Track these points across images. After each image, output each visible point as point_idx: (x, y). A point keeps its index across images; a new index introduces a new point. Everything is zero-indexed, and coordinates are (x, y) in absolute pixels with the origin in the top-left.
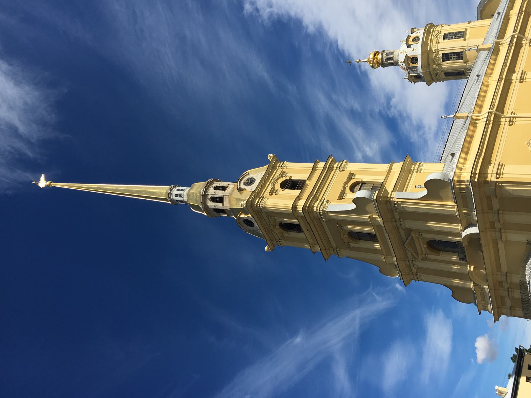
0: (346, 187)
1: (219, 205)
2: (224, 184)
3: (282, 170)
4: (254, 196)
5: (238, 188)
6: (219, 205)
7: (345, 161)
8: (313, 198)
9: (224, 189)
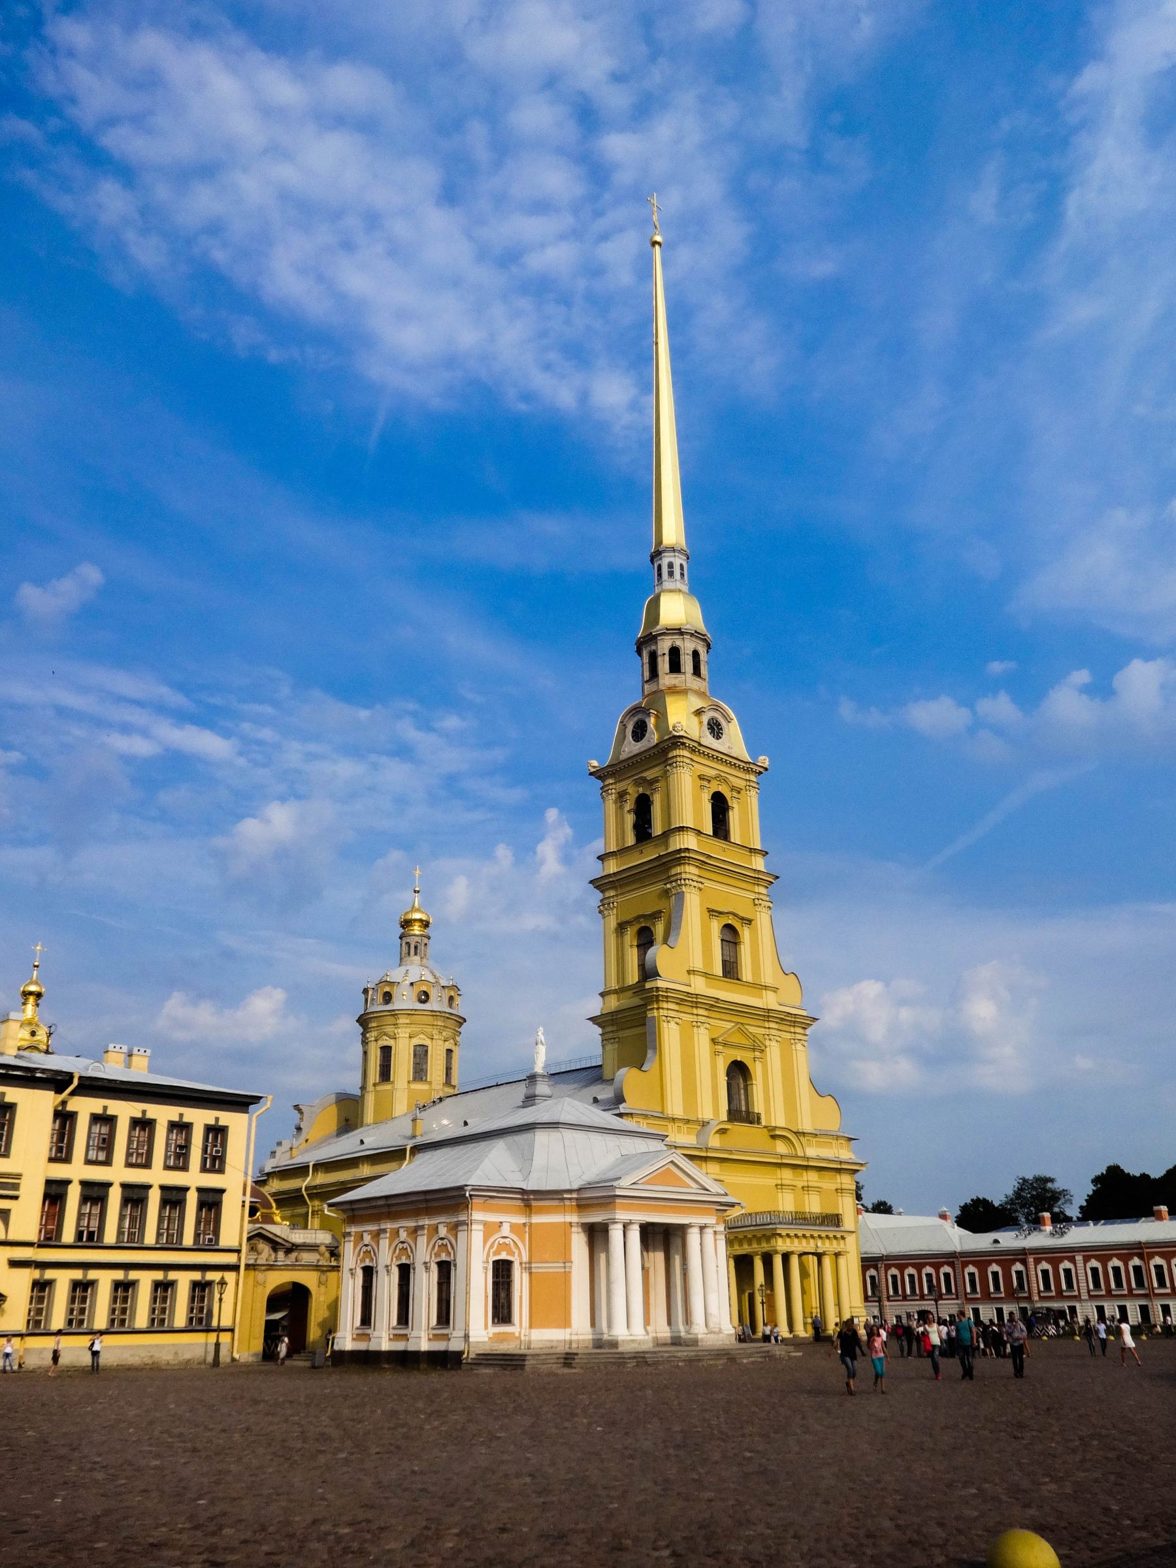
1: (664, 664)
3: (743, 788)
6: (664, 664)
8: (703, 862)
9: (697, 672)
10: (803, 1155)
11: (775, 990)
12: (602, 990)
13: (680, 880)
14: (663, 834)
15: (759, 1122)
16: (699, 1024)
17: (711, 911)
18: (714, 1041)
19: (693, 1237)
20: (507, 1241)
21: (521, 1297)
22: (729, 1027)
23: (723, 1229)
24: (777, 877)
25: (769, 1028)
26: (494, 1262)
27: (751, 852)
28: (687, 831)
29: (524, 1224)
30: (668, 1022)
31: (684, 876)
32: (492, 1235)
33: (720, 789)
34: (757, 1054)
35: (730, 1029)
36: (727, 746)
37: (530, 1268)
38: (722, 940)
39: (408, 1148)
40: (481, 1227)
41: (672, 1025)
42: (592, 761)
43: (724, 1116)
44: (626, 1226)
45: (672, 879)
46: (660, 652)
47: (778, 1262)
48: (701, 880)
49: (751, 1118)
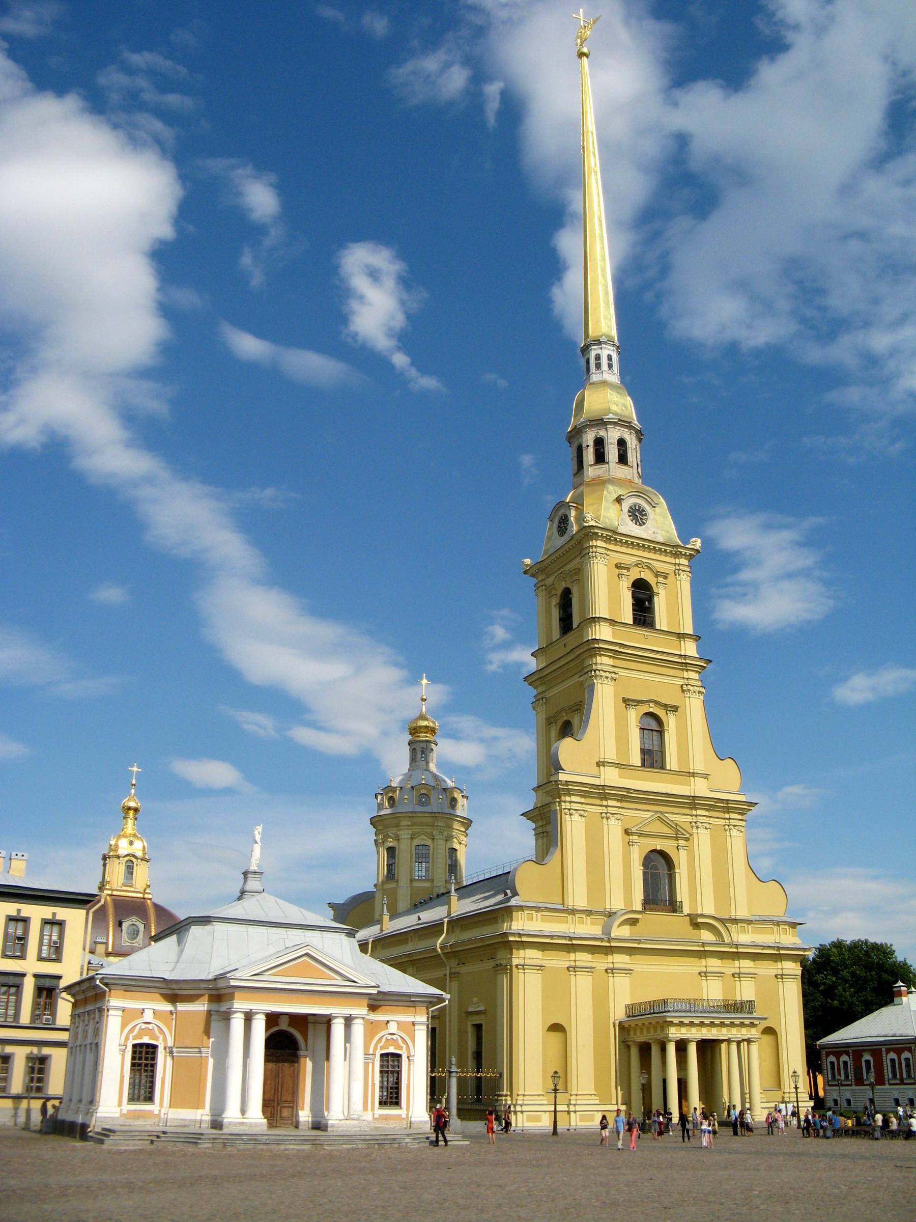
1: (589, 456)
2: (633, 456)
4: (608, 535)
5: (622, 497)
6: (589, 456)
7: (703, 690)
9: (623, 459)
10: (730, 942)
12: (536, 786)
13: (591, 671)
14: (578, 626)
15: (682, 912)
16: (609, 815)
18: (627, 832)
19: (338, 1028)
20: (150, 1026)
21: (163, 1079)
22: (648, 816)
23: (426, 1020)
24: (710, 661)
26: (135, 1046)
27: (679, 638)
29: (171, 1013)
31: (594, 667)
32: (130, 1022)
34: (681, 842)
35: (648, 818)
36: (651, 532)
37: (171, 1052)
38: (641, 728)
39: (370, 940)
40: (120, 1013)
41: (576, 817)
42: (525, 560)
44: (249, 1017)
45: (586, 671)
46: (584, 446)
47: (671, 1049)
49: (673, 907)
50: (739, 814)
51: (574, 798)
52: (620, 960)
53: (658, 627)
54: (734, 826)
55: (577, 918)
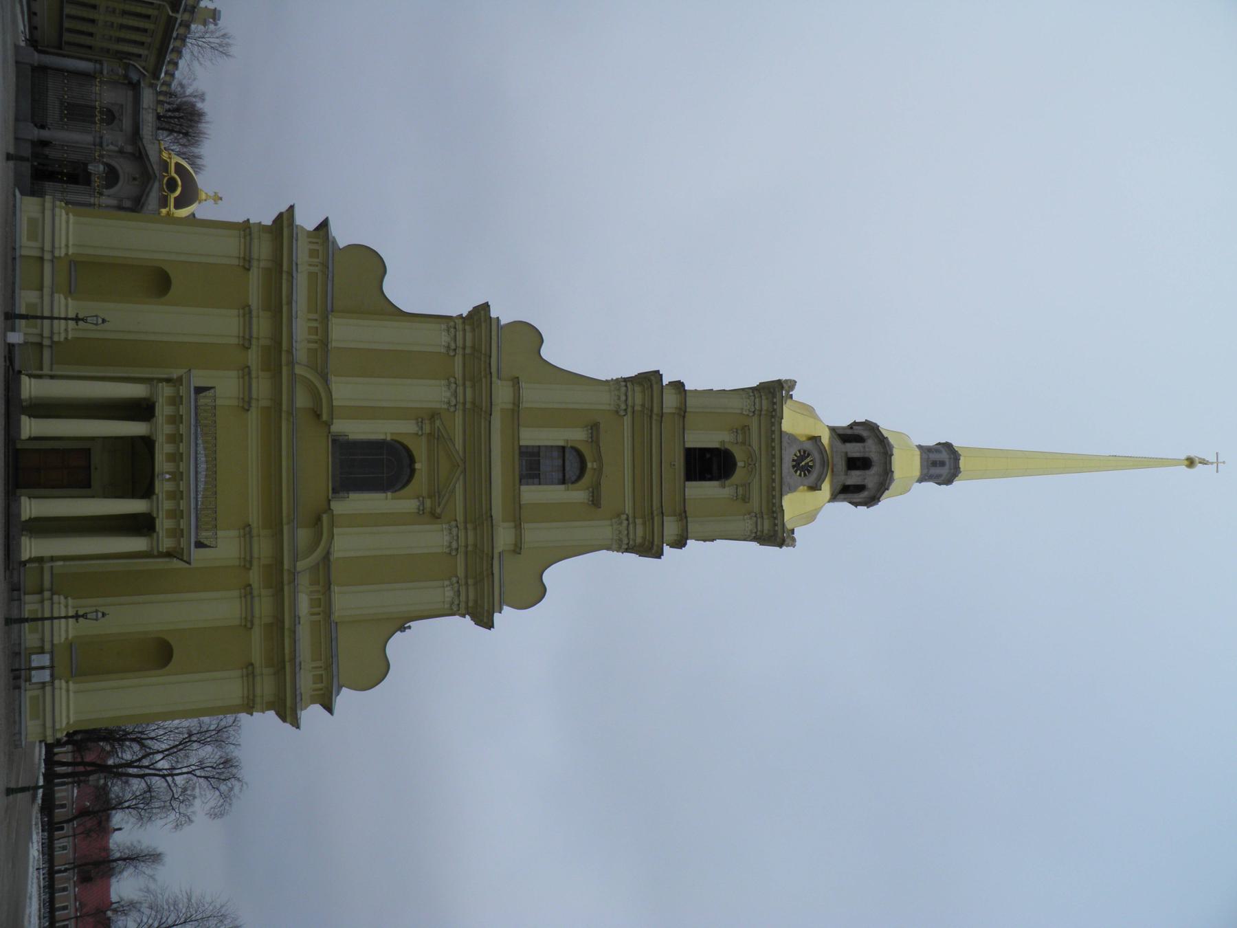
0: (595, 461)
2: (855, 478)
4: (776, 414)
8: (652, 411)
10: (298, 569)
11: (517, 549)
17: (594, 428)
18: (433, 415)
25: (466, 528)
27: (680, 515)
28: (680, 393)
30: (448, 331)
33: (740, 464)
34: (428, 503)
35: (454, 445)
38: (563, 448)
41: (445, 339)
43: (339, 426)
48: (629, 410)
50: (476, 601)
51: (469, 336)
52: (261, 387)
53: (687, 483)
54: (459, 591)
55: (318, 325)
